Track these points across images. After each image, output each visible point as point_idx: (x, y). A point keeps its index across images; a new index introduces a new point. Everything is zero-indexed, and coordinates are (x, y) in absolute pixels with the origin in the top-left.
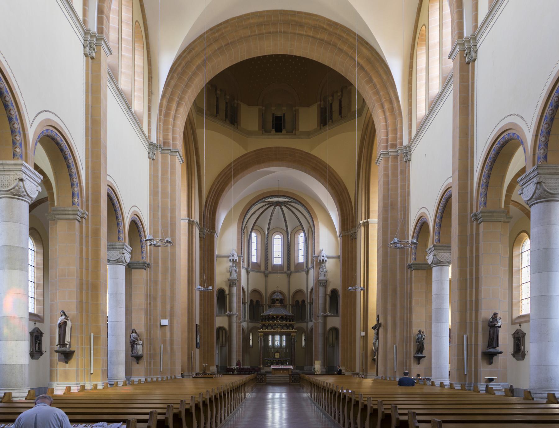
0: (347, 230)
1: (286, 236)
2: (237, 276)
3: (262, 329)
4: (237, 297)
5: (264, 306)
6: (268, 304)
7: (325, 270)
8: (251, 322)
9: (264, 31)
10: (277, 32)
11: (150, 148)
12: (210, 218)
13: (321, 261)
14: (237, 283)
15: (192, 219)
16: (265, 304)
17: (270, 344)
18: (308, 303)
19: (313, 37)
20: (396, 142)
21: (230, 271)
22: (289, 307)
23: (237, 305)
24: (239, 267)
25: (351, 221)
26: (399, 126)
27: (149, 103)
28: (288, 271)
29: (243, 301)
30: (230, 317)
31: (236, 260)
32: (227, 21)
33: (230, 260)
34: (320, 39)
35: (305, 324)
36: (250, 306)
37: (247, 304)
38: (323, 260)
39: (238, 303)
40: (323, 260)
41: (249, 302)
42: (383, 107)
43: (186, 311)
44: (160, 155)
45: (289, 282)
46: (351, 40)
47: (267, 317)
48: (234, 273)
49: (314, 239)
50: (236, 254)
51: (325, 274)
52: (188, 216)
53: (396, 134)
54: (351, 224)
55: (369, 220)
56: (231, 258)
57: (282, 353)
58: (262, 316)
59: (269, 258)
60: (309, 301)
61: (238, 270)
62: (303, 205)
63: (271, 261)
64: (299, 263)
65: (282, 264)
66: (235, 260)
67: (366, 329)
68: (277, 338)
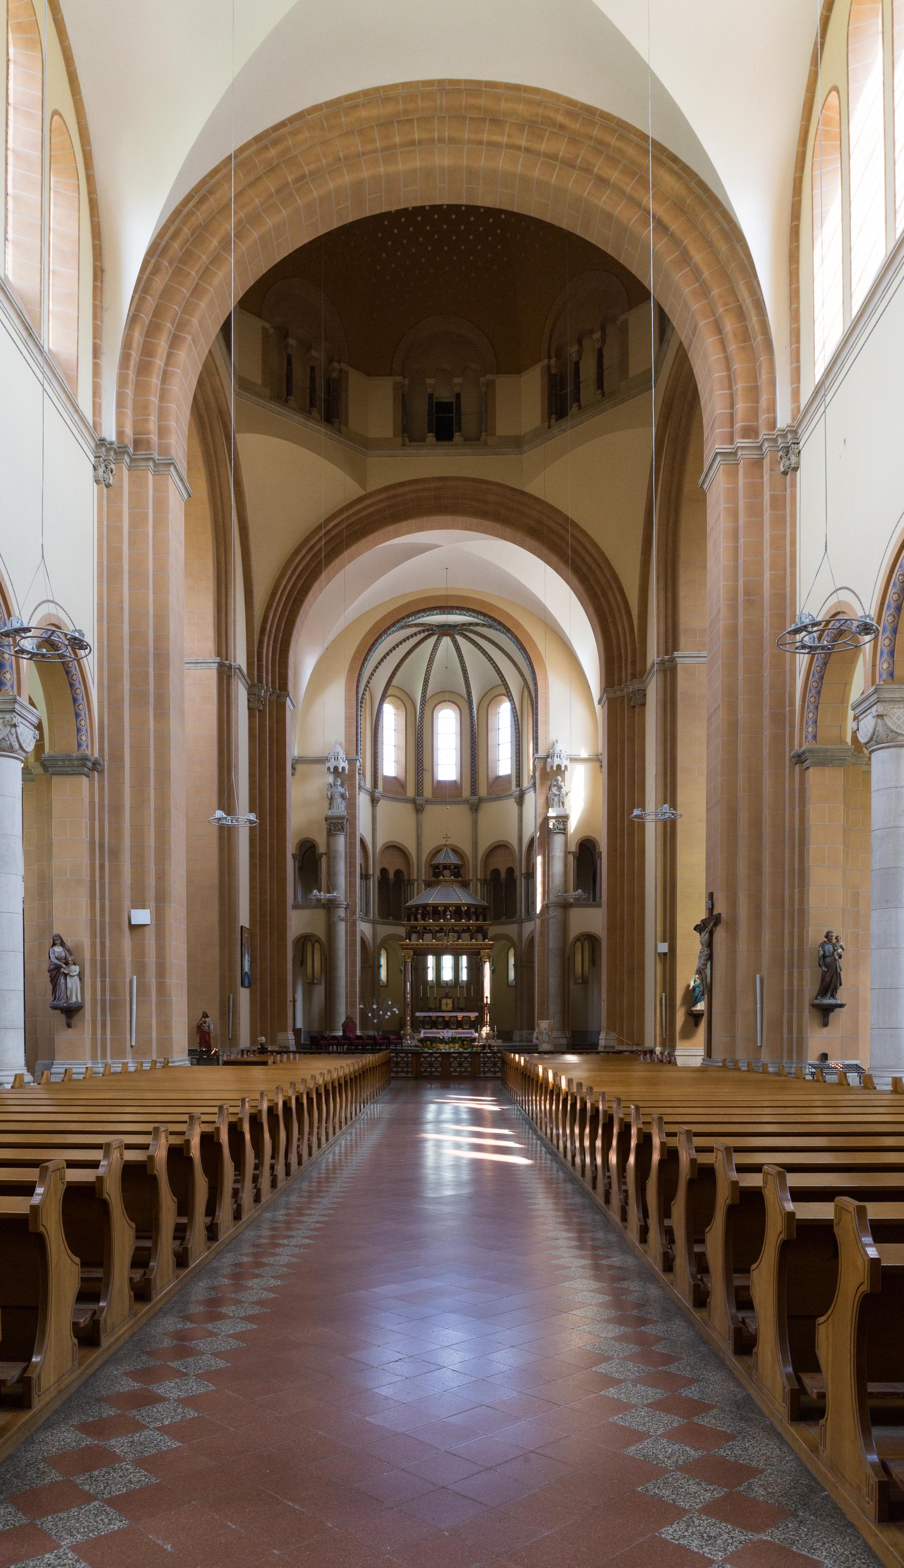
0: (620, 684)
2: (347, 809)
3: (410, 941)
4: (346, 862)
8: (383, 924)
9: (397, 140)
10: (432, 141)
11: (98, 455)
12: (273, 660)
14: (347, 826)
15: (227, 660)
16: (415, 878)
17: (431, 976)
18: (522, 875)
19: (527, 150)
20: (757, 420)
22: (477, 885)
23: (346, 881)
24: (352, 787)
25: (629, 659)
26: (764, 378)
27: (94, 337)
28: (473, 797)
29: (363, 872)
30: (330, 906)
31: (343, 768)
32: (299, 116)
33: (329, 768)
34: (546, 155)
35: (515, 926)
36: (380, 883)
38: (559, 766)
39: (350, 873)
41: (378, 873)
42: (718, 329)
43: (216, 892)
44: (126, 473)
45: (475, 823)
46: (631, 151)
49: (537, 715)
50: (342, 755)
52: (219, 654)
53: (757, 401)
54: (629, 667)
55: (676, 654)
56: (331, 764)
57: (458, 998)
58: (410, 908)
60: (524, 871)
62: (508, 630)
64: (498, 777)
65: (459, 781)
66: (340, 770)
67: (670, 934)
68: (447, 961)
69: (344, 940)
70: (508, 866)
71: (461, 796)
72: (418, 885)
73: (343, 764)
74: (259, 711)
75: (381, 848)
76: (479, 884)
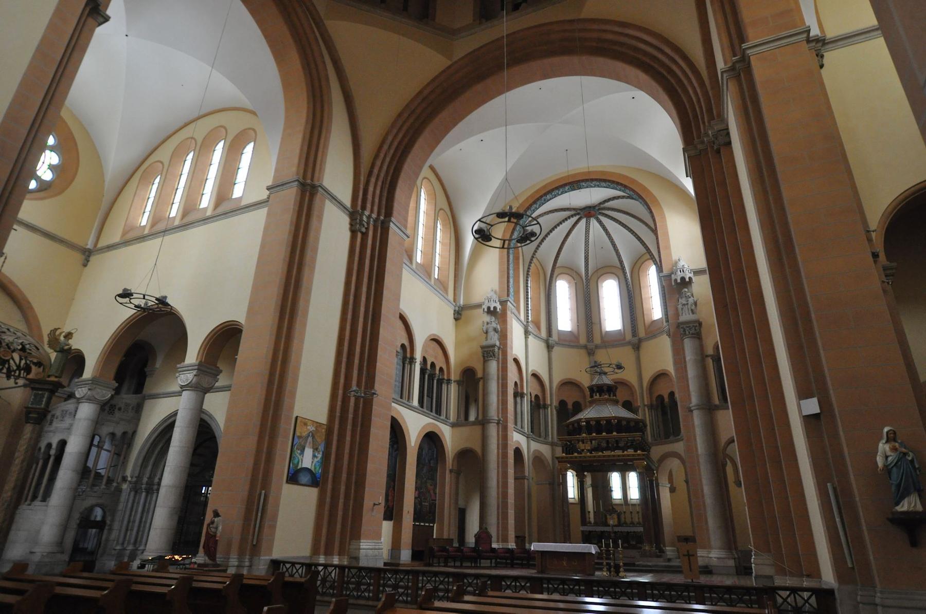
1: (620, 273)
2: (499, 340)
7: (691, 300)
13: (679, 281)
17: (617, 494)
22: (644, 410)
30: (483, 422)
31: (495, 308)
37: (549, 409)
38: (683, 279)
40: (683, 279)
47: (576, 425)
48: (492, 333)
50: (495, 297)
51: (693, 307)
55: (744, 46)
56: (485, 307)
59: (595, 320)
61: (499, 327)
63: (599, 325)
64: (654, 321)
69: (496, 451)
70: (669, 391)
71: (624, 339)
74: (363, 233)
76: (646, 409)
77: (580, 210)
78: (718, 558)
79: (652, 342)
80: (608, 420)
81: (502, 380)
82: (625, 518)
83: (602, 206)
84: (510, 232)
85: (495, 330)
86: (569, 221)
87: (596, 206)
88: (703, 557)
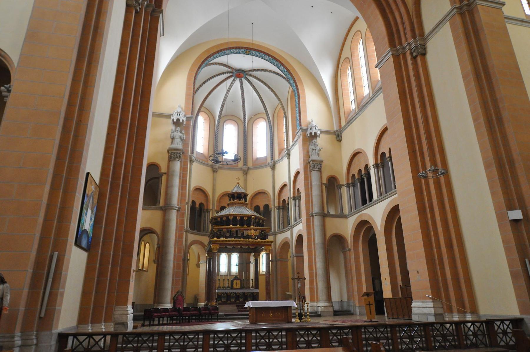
4: (180, 179)
5: (211, 212)
6: (216, 209)
13: (313, 134)
16: (211, 208)
18: (275, 207)
21: (172, 138)
23: (179, 192)
30: (166, 209)
38: (315, 133)
40: (315, 133)
41: (190, 203)
45: (246, 181)
47: (224, 219)
50: (182, 113)
60: (276, 205)
64: (258, 158)
72: (212, 213)
73: (182, 118)
74: (136, 12)
75: (193, 189)
77: (235, 70)
78: (324, 306)
79: (257, 172)
80: (242, 217)
81: (183, 177)
82: (219, 284)
83: (251, 73)
84: (197, 68)
85: (181, 137)
86: (222, 75)
87: (246, 71)
88: (313, 306)
